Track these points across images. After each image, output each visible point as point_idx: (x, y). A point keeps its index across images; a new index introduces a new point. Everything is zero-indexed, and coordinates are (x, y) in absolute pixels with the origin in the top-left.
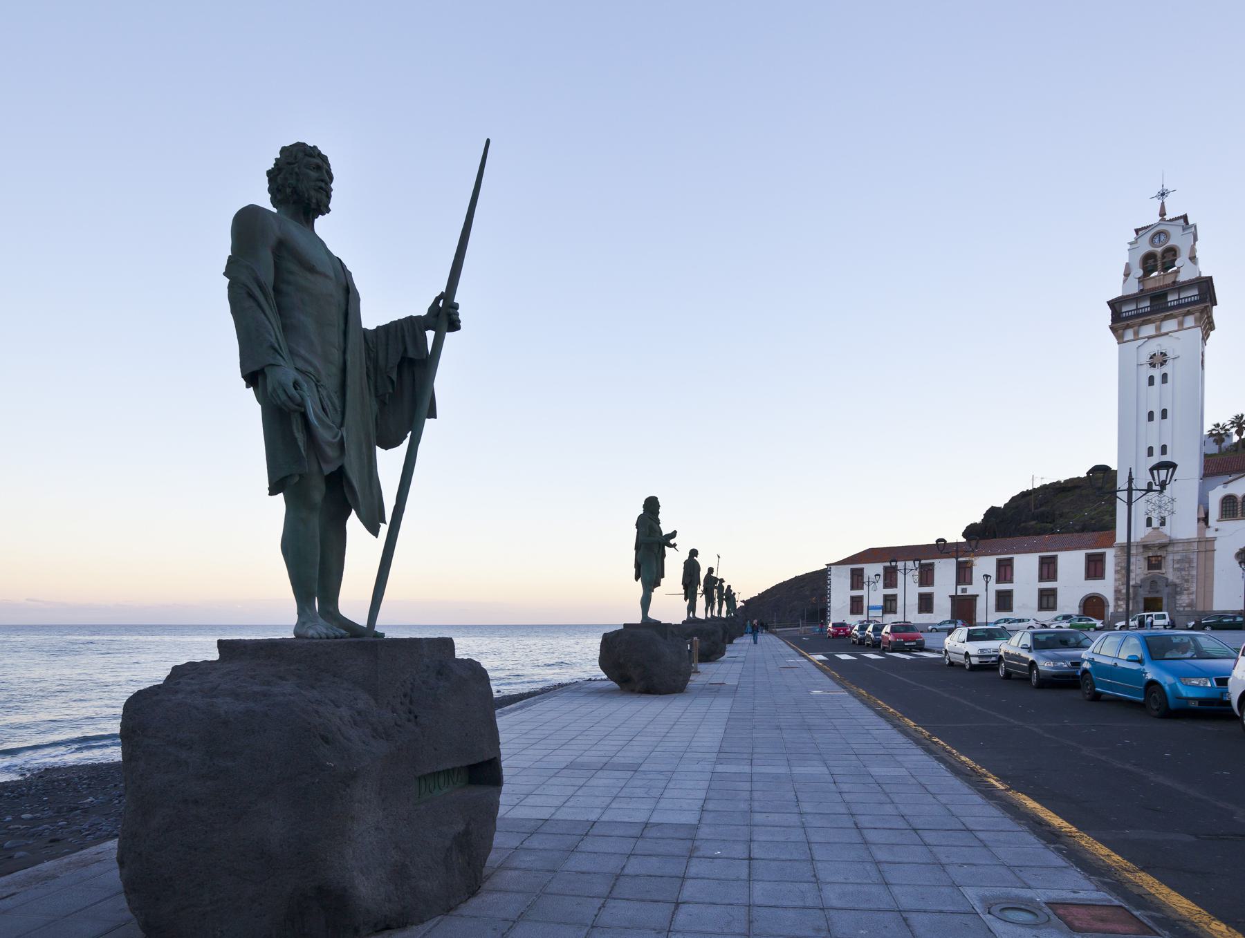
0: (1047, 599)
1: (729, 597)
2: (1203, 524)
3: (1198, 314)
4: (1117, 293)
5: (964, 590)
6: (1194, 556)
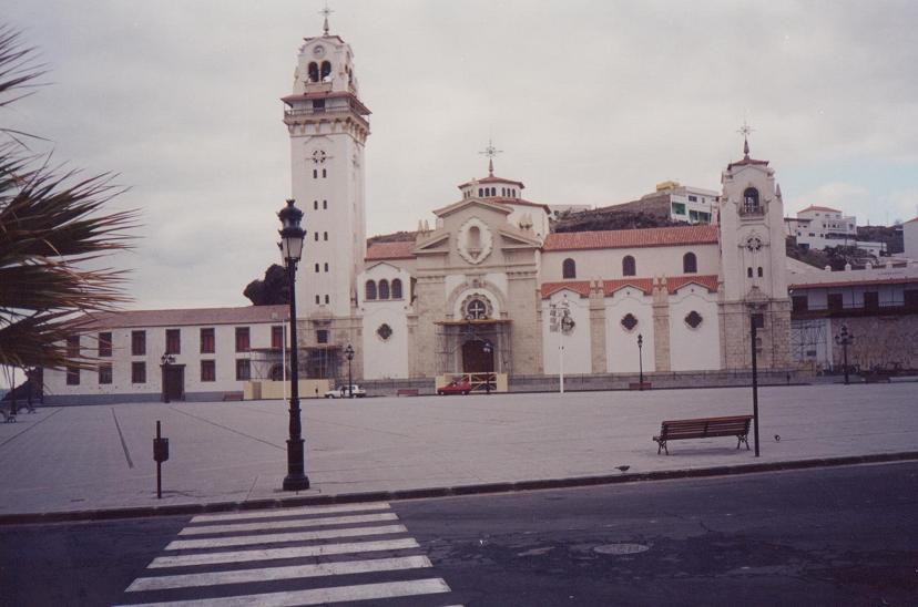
3: (344, 123)
4: (289, 93)
6: (349, 332)
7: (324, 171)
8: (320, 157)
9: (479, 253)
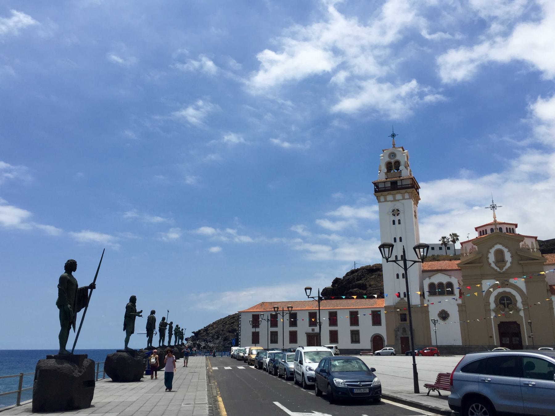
0: (355, 337)
1: (179, 334)
2: (423, 297)
5: (313, 330)
7: (399, 220)
8: (396, 212)
9: (504, 266)
